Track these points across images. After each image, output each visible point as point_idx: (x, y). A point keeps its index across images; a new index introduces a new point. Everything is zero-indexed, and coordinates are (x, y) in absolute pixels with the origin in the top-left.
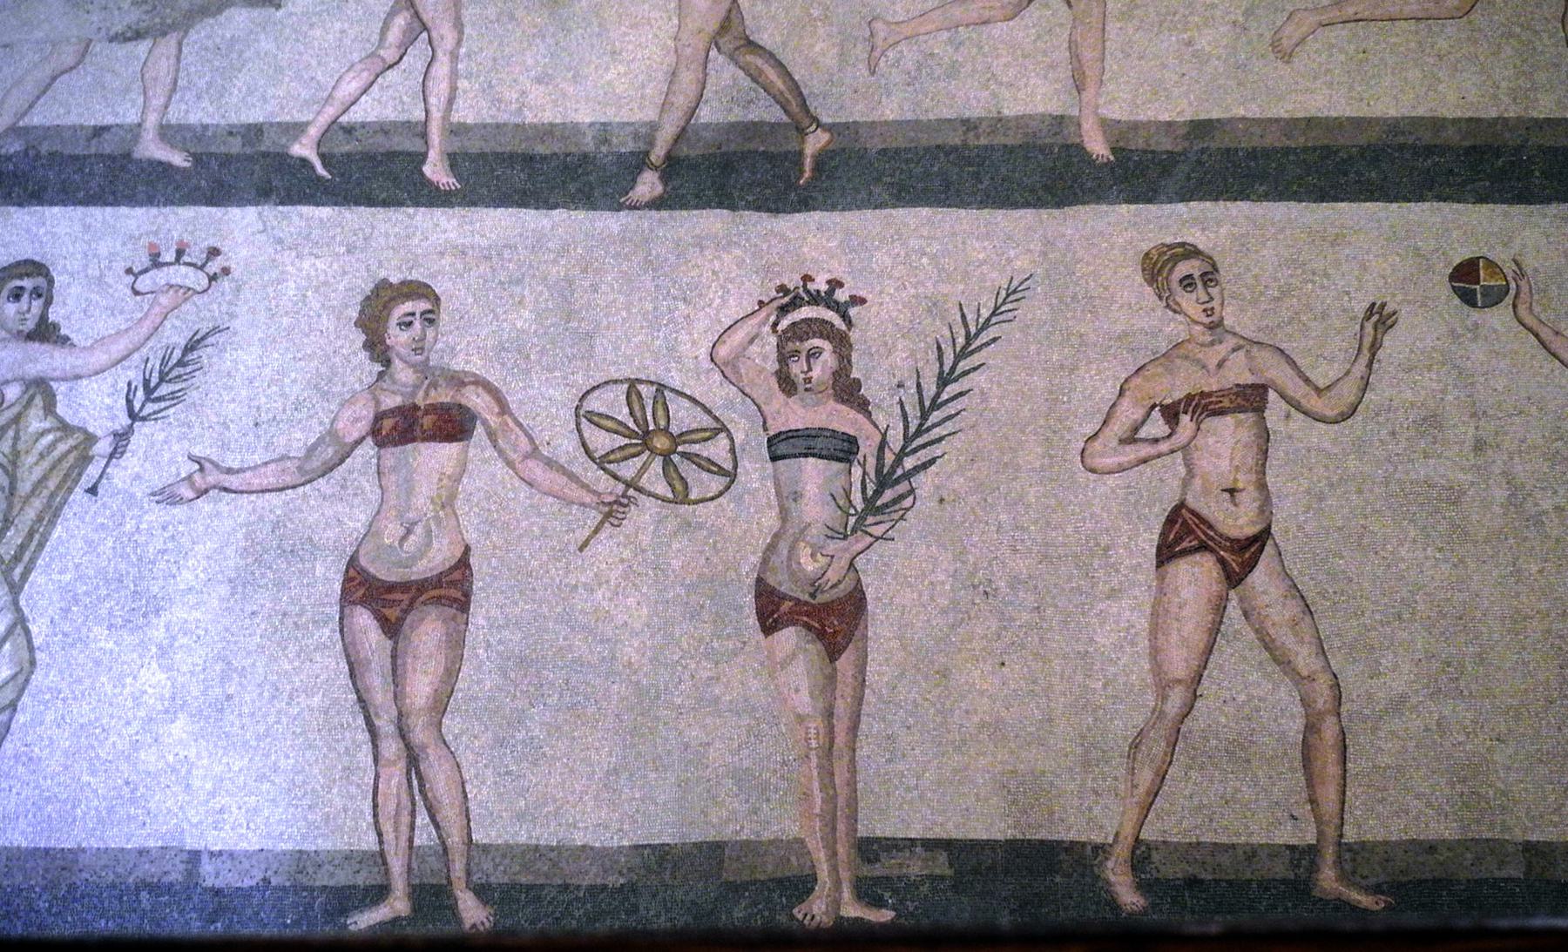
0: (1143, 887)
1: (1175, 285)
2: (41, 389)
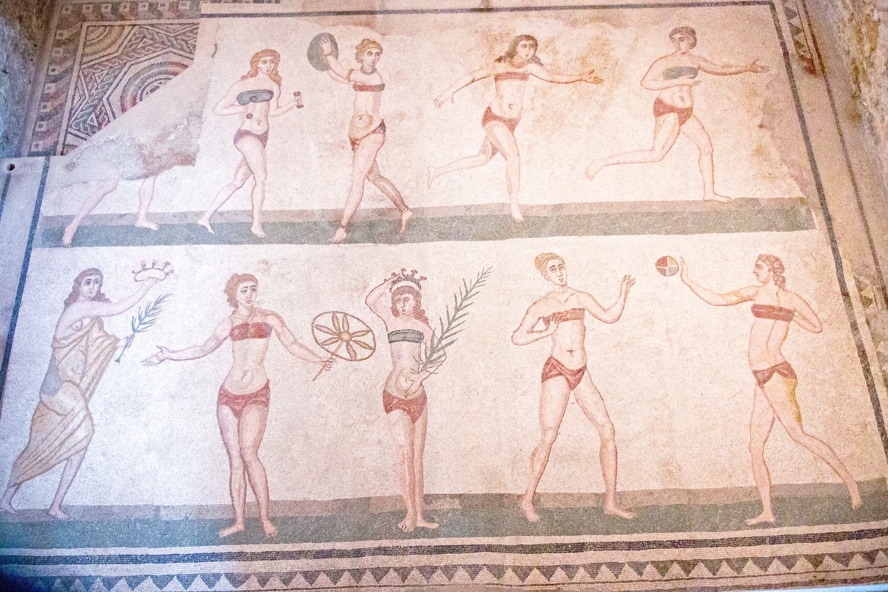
0: (537, 511)
1: (548, 269)
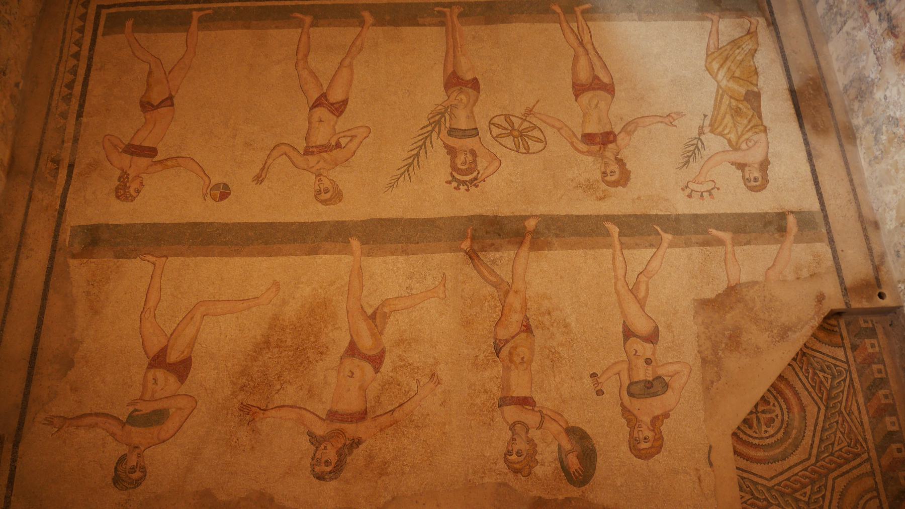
1: (331, 190)
2: (736, 148)
